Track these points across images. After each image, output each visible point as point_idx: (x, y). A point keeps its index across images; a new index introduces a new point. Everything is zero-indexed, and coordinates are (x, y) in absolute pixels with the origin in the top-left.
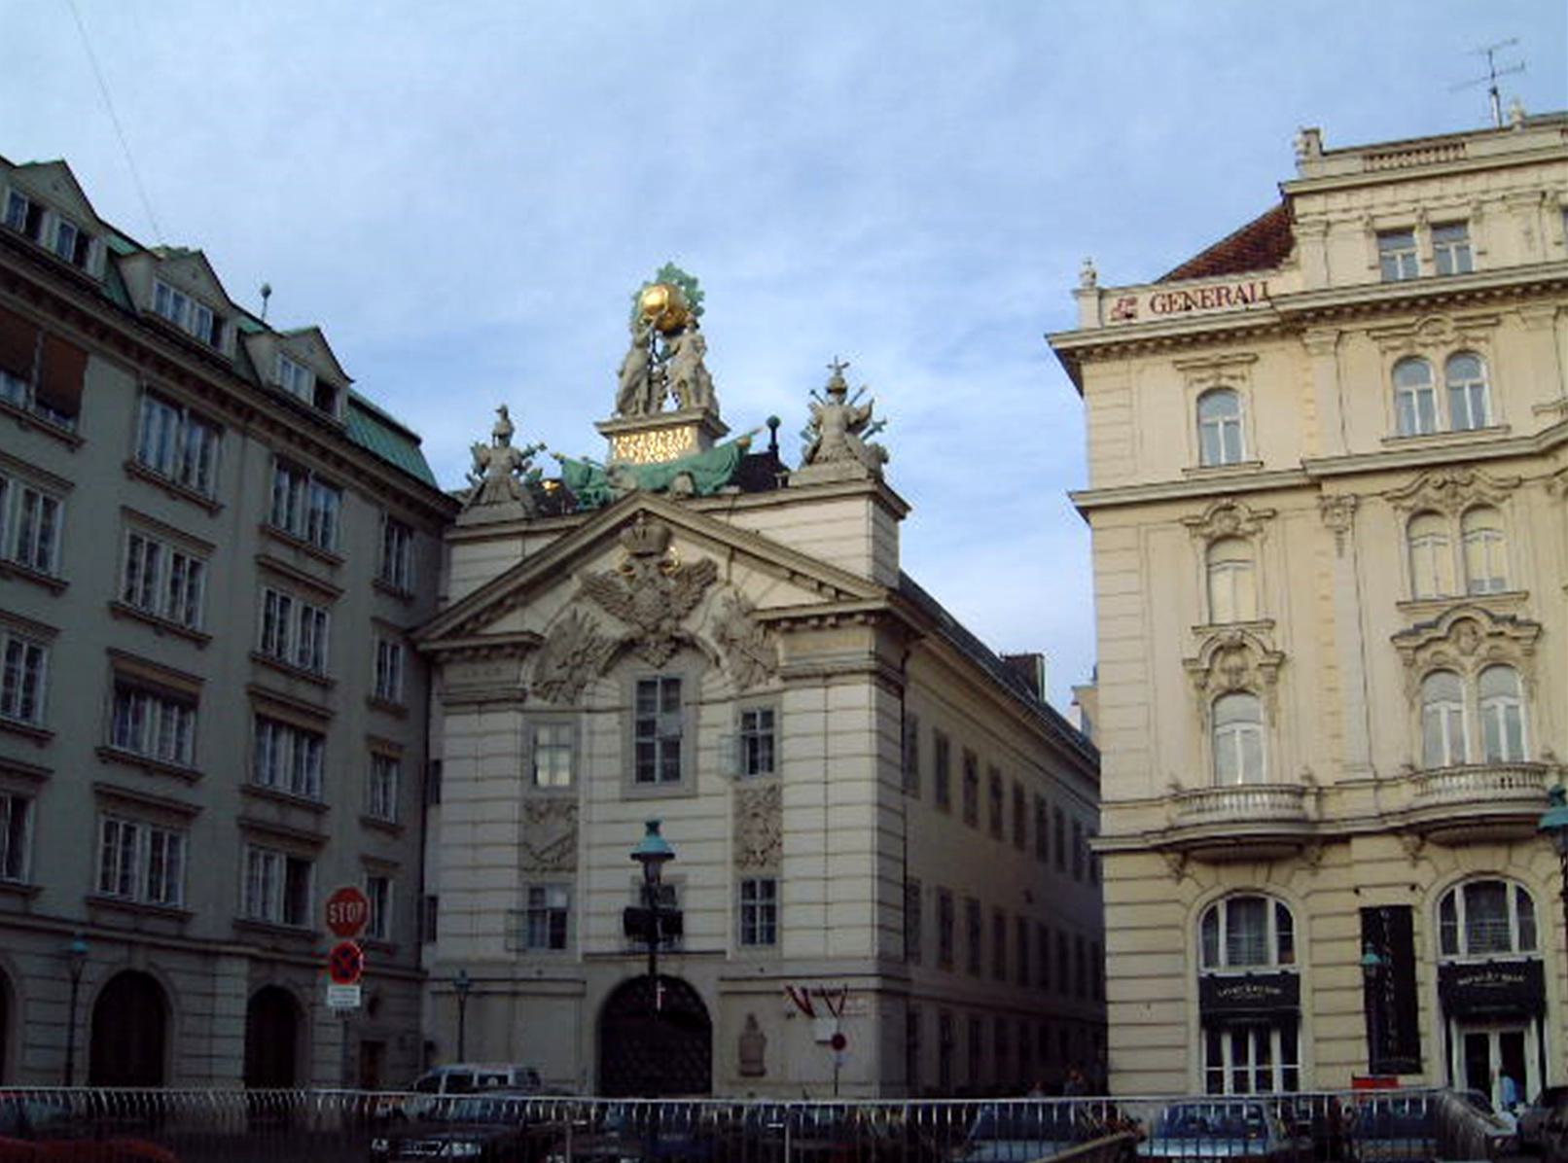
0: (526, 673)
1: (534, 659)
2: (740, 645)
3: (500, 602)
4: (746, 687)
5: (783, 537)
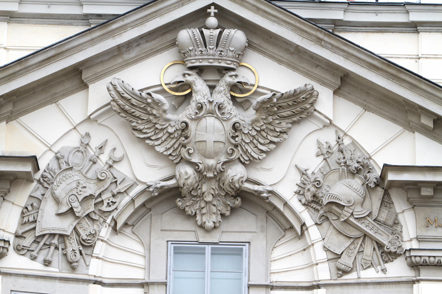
2: (345, 214)
4: (345, 272)
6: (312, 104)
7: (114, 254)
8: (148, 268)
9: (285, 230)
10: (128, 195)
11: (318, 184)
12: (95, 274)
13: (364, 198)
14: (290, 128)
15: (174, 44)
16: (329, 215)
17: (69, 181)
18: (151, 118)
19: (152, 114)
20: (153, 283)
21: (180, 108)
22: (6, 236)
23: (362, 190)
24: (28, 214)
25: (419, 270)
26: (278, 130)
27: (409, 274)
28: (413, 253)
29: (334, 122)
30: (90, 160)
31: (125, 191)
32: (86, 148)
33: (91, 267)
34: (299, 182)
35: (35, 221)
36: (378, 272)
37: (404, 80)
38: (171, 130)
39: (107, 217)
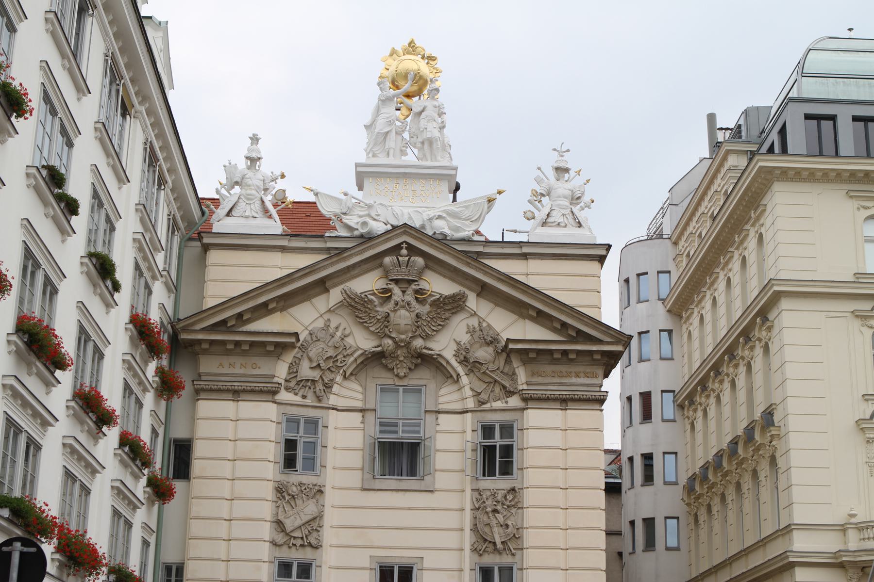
0: (281, 370)
1: (289, 357)
2: (484, 368)
3: (265, 304)
4: (483, 403)
5: (534, 282)
6: (464, 302)
7: (344, 392)
8: (364, 401)
9: (447, 378)
10: (353, 356)
11: (467, 350)
12: (332, 404)
13: (495, 359)
14: (450, 316)
15: (381, 265)
16: (473, 369)
17: (317, 348)
18: (367, 310)
19: (368, 308)
20: (368, 410)
21: (384, 305)
22: (280, 381)
23: (493, 354)
24: (293, 367)
25: (527, 402)
26: (443, 317)
27: (521, 404)
28: (524, 392)
29: (478, 313)
30: (330, 335)
31: (351, 354)
32: (328, 328)
33: (330, 400)
34: (456, 349)
35: (297, 372)
36: (503, 403)
37: (519, 288)
38: (379, 317)
39: (340, 369)
